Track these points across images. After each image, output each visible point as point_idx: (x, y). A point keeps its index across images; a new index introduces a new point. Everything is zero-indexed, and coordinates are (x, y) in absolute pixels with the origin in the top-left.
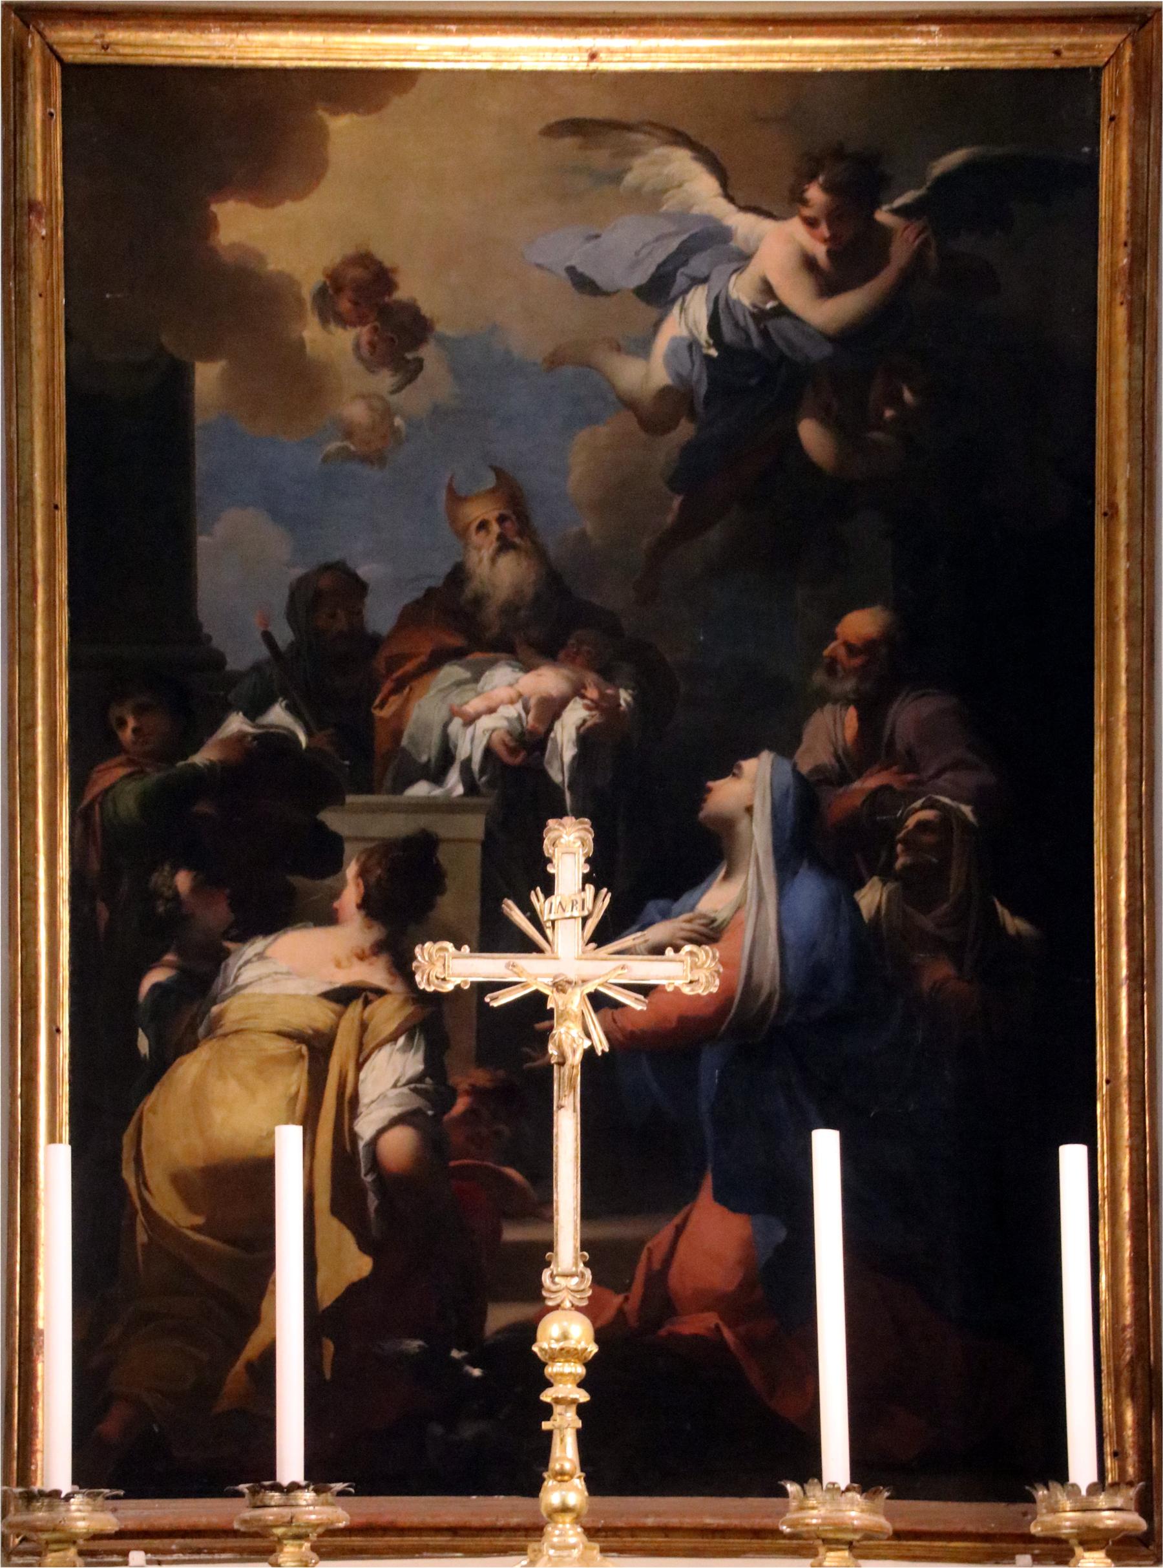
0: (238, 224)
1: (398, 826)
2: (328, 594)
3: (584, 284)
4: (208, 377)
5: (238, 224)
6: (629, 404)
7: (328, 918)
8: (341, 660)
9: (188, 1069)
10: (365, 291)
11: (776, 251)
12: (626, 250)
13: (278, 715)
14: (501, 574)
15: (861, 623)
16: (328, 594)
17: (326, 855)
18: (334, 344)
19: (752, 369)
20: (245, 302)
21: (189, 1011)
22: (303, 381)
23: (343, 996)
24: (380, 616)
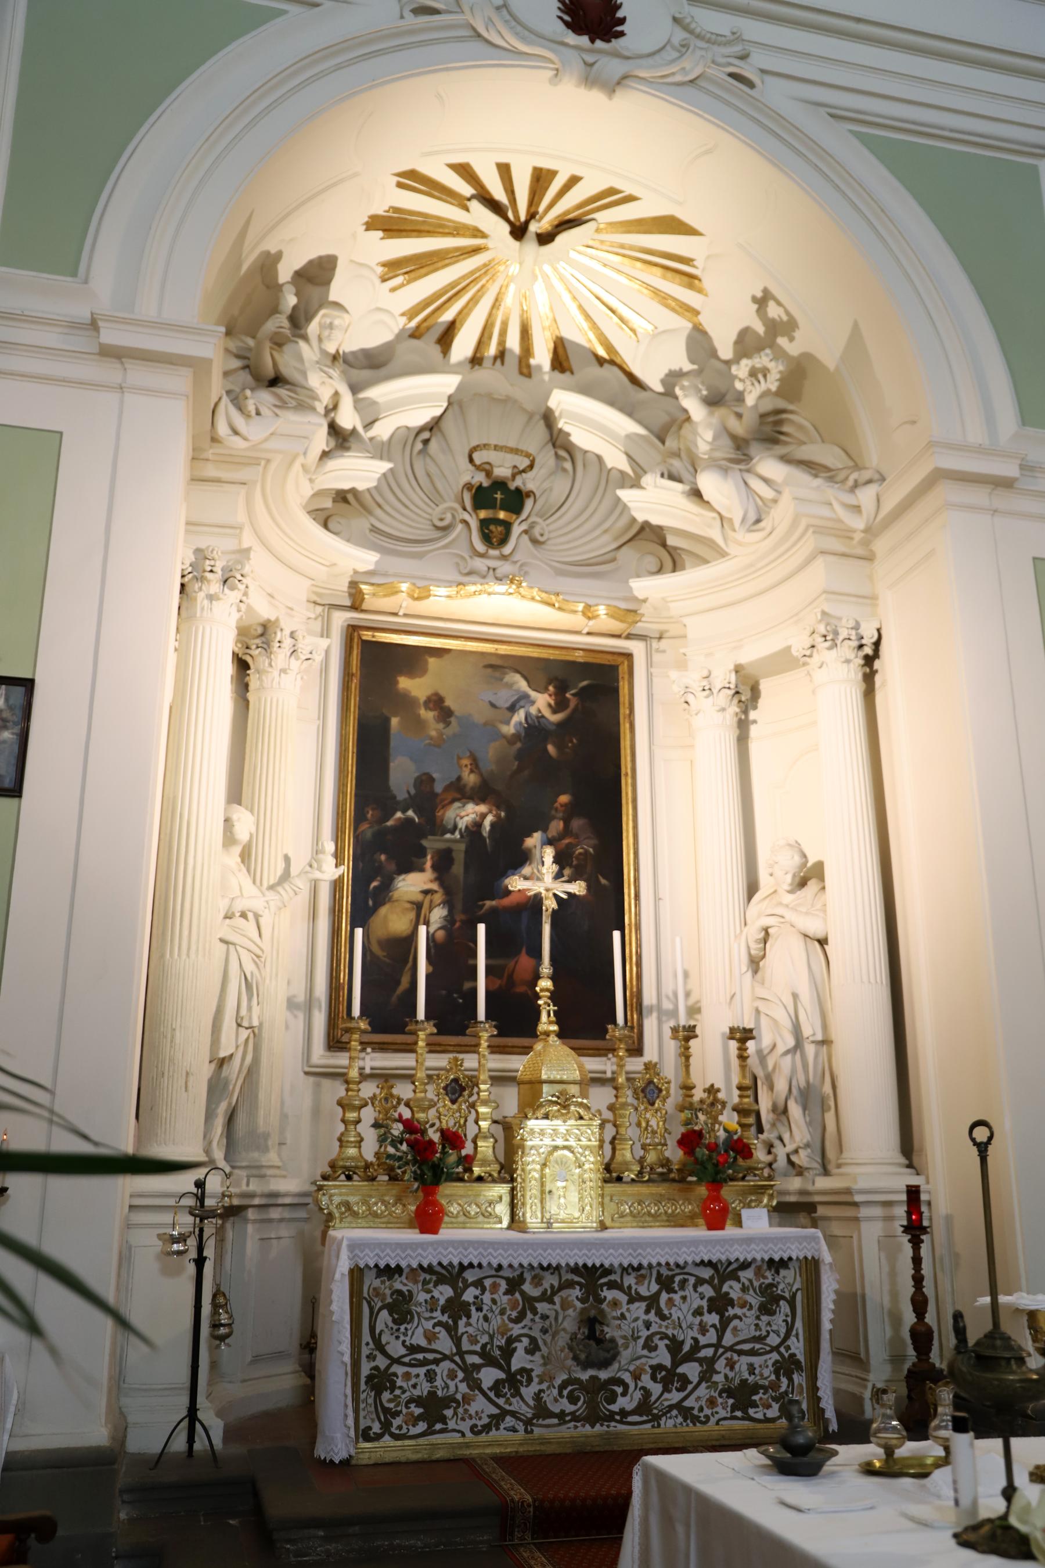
0: (404, 683)
1: (441, 846)
2: (425, 781)
3: (493, 705)
4: (395, 721)
5: (404, 683)
6: (504, 737)
7: (422, 870)
8: (427, 799)
9: (383, 910)
10: (436, 702)
11: (542, 702)
12: (504, 698)
13: (410, 813)
14: (471, 779)
15: (564, 799)
16: (425, 781)
17: (422, 852)
18: (428, 715)
19: (535, 730)
20: (406, 703)
21: (383, 895)
22: (420, 724)
23: (426, 892)
24: (438, 788)
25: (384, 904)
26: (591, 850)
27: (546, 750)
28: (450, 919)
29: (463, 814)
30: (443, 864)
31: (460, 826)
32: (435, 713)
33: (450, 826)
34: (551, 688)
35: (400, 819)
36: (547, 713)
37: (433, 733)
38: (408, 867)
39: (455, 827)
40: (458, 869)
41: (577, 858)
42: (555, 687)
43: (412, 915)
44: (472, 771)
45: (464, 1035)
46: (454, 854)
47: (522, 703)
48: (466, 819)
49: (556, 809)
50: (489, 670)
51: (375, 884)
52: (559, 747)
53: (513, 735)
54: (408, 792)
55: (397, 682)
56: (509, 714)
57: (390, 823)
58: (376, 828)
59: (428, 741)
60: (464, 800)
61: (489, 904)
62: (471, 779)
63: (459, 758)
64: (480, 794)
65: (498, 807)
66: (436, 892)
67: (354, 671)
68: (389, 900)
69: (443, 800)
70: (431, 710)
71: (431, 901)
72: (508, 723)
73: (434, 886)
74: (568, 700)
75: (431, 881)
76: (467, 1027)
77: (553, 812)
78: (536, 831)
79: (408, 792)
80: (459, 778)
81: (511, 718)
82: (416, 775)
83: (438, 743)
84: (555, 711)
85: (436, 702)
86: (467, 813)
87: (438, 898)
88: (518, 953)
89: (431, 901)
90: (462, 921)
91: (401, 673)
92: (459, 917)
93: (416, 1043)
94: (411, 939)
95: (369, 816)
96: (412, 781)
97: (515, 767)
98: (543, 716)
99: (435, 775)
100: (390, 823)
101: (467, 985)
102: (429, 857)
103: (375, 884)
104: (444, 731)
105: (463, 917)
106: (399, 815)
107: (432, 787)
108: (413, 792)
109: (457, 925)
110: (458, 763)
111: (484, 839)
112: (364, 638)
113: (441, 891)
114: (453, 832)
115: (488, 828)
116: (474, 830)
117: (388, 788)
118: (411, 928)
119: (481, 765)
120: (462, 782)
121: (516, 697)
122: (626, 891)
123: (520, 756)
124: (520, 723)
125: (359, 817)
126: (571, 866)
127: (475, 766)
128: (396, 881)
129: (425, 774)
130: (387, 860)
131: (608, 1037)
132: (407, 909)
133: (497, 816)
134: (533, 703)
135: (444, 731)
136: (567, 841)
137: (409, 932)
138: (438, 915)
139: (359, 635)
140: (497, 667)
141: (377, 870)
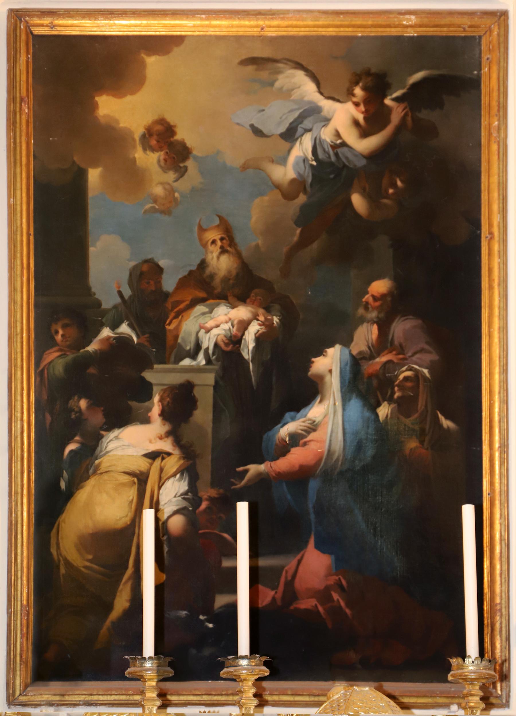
1: (176, 379)
2: (147, 273)
3: (257, 132)
4: (94, 175)
6: (278, 187)
7: (146, 421)
8: (152, 304)
10: (161, 134)
11: (342, 118)
12: (276, 117)
13: (124, 329)
14: (222, 264)
15: (380, 286)
16: (147, 273)
17: (145, 391)
18: (149, 160)
19: (331, 171)
20: (110, 142)
23: (153, 456)
24: (169, 283)
25: (88, 478)
26: (426, 371)
27: (349, 203)
28: (192, 496)
29: (210, 324)
30: (180, 407)
31: (204, 346)
32: (160, 155)
33: (189, 346)
34: (358, 91)
35: (108, 338)
36: (351, 137)
37: (159, 191)
38: (120, 417)
39: (198, 346)
40: (203, 415)
41: (401, 387)
42: (364, 89)
43: (132, 493)
44: (223, 250)
45: (218, 678)
46: (197, 392)
47: (307, 123)
48: (215, 331)
49: (366, 306)
50: (250, 69)
51: (72, 447)
52: (373, 197)
53: (293, 181)
54: (120, 293)
55: (95, 106)
56: (284, 145)
57: (92, 347)
58: (71, 356)
59: (148, 206)
60: (211, 301)
61: (253, 469)
62: (222, 264)
63: (202, 230)
64: (243, 287)
65: (268, 309)
66: (169, 454)
67: (24, 93)
68: (95, 473)
69: (178, 303)
70: (153, 150)
71: (161, 470)
72: (283, 161)
73: (167, 445)
74: (389, 110)
75: (161, 438)
76: (222, 666)
77: (361, 311)
78: (332, 345)
79: (120, 293)
80: (203, 264)
81: (289, 151)
82: (133, 263)
83: (167, 206)
84: (364, 134)
85: (161, 134)
86: (215, 323)
87: (173, 463)
88: (300, 546)
89: (161, 470)
90: (211, 499)
91: (101, 89)
92: (207, 492)
93: (142, 693)
94: (134, 526)
95: (59, 338)
96: (126, 276)
97: (296, 239)
98: (344, 144)
99: (162, 263)
100: (92, 347)
101: (221, 601)
102: (156, 399)
103: (72, 447)
104: (175, 185)
105: (213, 493)
106: (106, 332)
107: (158, 283)
108: (127, 292)
109: (204, 505)
110: (201, 239)
111: (246, 362)
112: (36, 33)
113: (176, 452)
114: (194, 356)
115: (251, 345)
116: (228, 352)
117: (87, 290)
118: (131, 515)
119: (238, 239)
120: (208, 271)
121: (296, 114)
122: (485, 437)
123: (304, 218)
124: (305, 160)
125: (43, 340)
126: (390, 400)
127: (229, 241)
128: (105, 441)
129: (146, 261)
130: (89, 407)
131: (450, 678)
132: (123, 485)
133: (267, 324)
134: (327, 120)
135: (175, 185)
136: (383, 359)
137: (127, 520)
138: (172, 492)
139: (28, 26)
140: (261, 60)
141: (73, 425)
